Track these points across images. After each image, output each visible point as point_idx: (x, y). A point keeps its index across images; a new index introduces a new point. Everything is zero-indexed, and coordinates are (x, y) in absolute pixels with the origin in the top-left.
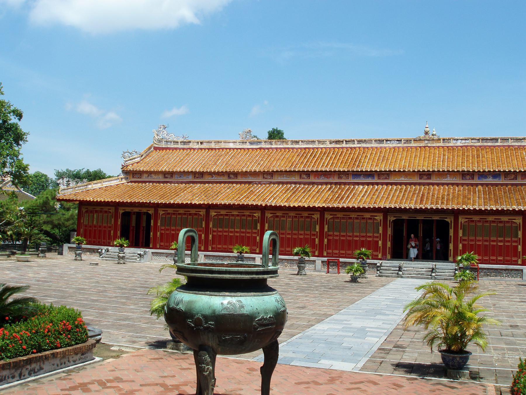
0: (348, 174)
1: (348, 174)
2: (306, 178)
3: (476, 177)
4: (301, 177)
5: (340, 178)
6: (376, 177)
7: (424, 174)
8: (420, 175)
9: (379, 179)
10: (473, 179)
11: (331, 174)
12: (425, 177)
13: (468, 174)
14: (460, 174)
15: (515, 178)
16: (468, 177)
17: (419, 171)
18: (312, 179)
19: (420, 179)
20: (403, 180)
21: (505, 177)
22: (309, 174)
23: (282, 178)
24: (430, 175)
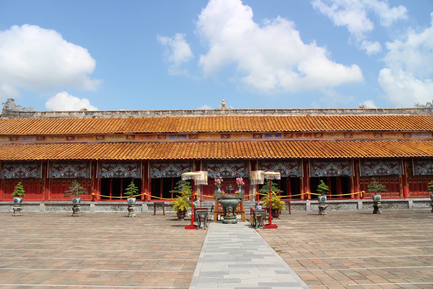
0: (166, 135)
1: (166, 135)
2: (132, 138)
3: (263, 136)
4: (127, 138)
5: (159, 138)
6: (188, 137)
7: (225, 135)
8: (222, 135)
9: (190, 138)
10: (261, 137)
11: (152, 135)
12: (225, 137)
13: (257, 134)
14: (251, 134)
15: (292, 136)
16: (257, 136)
17: (221, 132)
18: (137, 139)
19: (222, 138)
20: (208, 138)
21: (284, 136)
22: (134, 136)
23: (112, 139)
24: (229, 135)
